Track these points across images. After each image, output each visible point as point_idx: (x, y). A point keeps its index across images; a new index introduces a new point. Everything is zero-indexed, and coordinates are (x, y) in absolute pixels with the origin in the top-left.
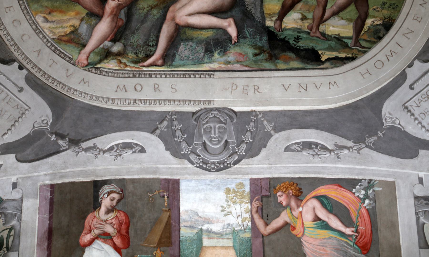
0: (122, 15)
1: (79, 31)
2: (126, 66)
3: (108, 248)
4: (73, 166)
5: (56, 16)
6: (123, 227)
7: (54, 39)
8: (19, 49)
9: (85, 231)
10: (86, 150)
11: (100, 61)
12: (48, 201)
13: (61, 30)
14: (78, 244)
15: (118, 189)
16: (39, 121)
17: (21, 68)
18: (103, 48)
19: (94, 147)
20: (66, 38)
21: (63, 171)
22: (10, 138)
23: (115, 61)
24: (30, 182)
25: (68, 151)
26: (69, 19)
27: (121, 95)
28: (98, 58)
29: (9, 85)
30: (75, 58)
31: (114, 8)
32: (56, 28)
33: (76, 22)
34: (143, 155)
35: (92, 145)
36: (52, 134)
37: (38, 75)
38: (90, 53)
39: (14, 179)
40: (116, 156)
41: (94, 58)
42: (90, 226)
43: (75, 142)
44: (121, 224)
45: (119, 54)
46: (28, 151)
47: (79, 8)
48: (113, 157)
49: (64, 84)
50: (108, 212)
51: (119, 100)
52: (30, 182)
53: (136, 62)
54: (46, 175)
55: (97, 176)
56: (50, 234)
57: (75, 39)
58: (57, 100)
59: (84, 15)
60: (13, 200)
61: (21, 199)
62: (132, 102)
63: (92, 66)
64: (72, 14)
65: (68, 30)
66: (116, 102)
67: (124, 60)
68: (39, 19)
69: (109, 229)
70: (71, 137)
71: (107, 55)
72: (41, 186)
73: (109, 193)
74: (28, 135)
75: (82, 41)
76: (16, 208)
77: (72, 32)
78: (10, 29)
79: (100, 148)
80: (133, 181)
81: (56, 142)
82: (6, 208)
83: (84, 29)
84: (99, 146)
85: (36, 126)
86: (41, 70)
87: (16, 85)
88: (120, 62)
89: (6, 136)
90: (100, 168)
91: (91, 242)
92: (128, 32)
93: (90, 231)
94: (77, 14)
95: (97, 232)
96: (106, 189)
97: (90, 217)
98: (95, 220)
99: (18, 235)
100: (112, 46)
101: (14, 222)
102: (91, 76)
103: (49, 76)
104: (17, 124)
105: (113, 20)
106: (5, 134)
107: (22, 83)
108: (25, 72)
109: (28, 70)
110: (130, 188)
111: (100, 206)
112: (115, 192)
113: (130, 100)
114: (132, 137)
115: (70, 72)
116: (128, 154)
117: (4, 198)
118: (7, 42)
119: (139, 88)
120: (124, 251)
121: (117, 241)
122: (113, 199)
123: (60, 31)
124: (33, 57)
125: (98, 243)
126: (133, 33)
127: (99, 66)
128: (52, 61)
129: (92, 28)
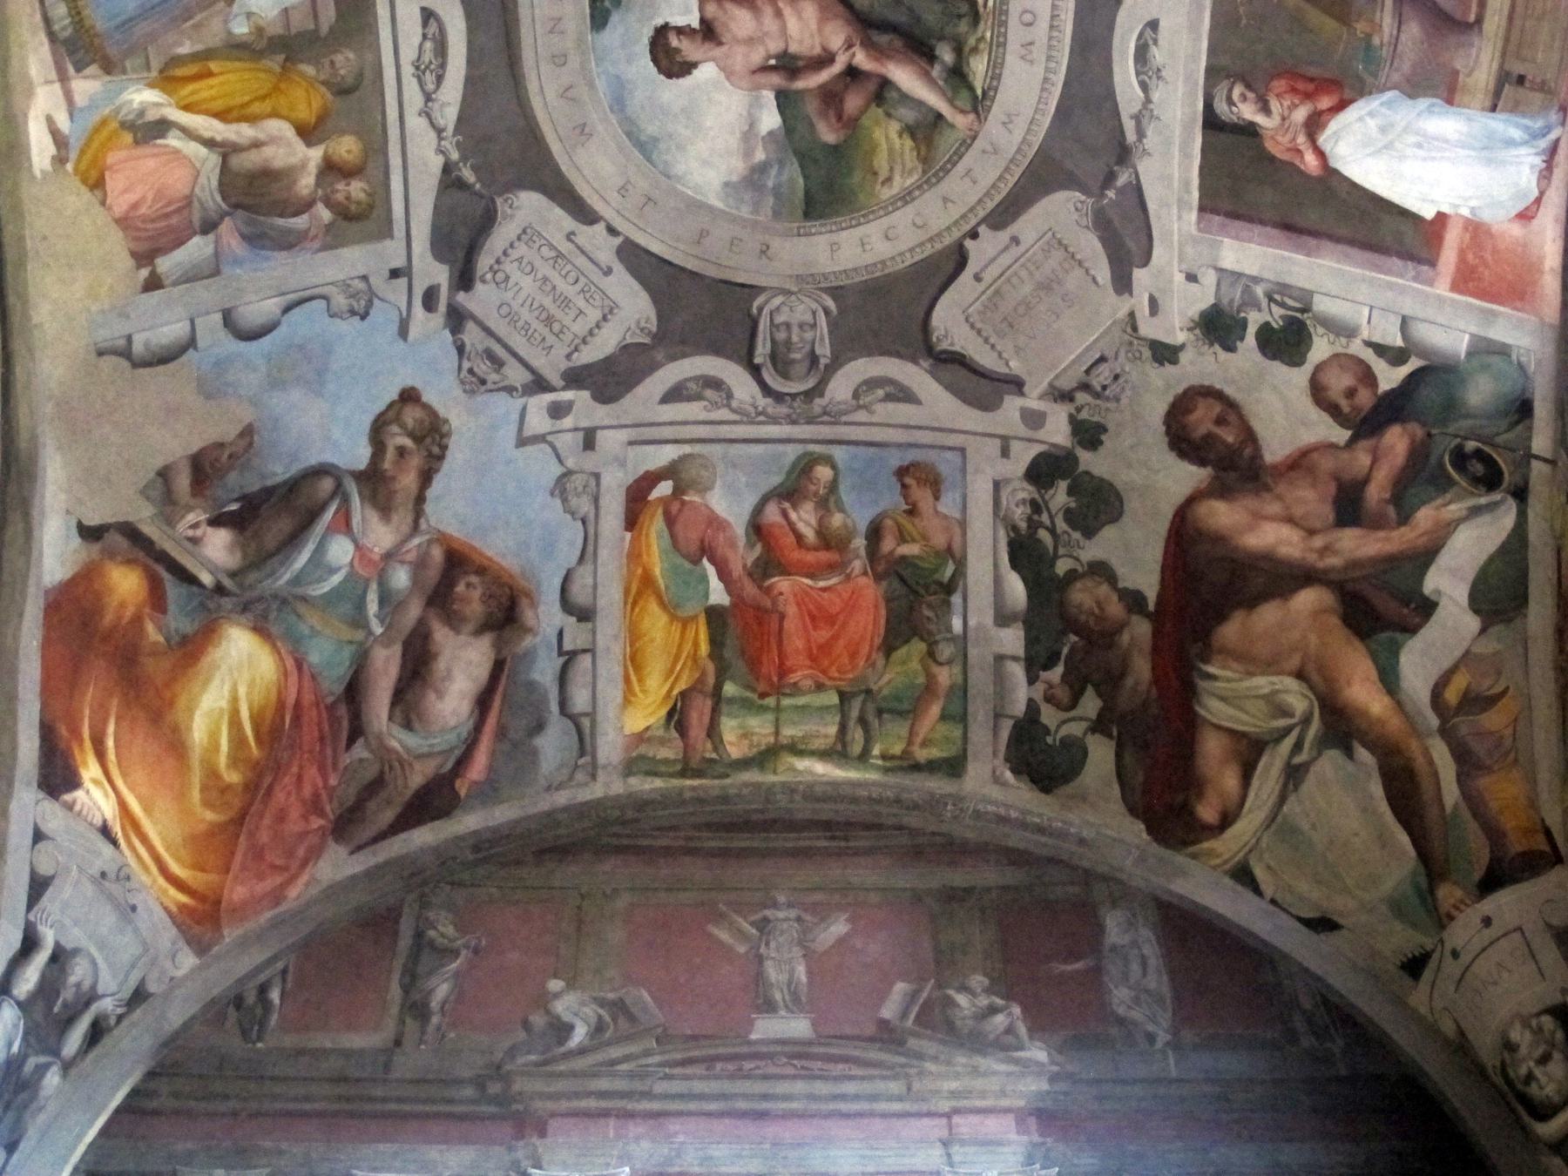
0: (883, 39)
1: (911, 123)
2: (982, 38)
3: (1335, 124)
4: (1170, 168)
5: (881, 162)
6: (1301, 86)
7: (924, 172)
8: (939, 235)
9: (1297, 162)
10: (1141, 134)
11: (971, 89)
12: (1227, 221)
13: (907, 156)
14: (1319, 179)
15: (1225, 84)
16: (1076, 216)
17: (974, 235)
18: (946, 81)
19: (1137, 118)
20: (923, 149)
21: (1176, 184)
22: (1103, 273)
23: (972, 60)
24: (1189, 250)
25: (1140, 169)
26: (887, 137)
27: (1039, 54)
28: (965, 94)
29: (1005, 260)
30: (961, 135)
31: (868, 56)
32: (904, 165)
33: (894, 127)
34: (1162, 24)
35: (1133, 122)
36: (1103, 195)
37: (990, 205)
38: (955, 107)
39: (1179, 278)
40: (1159, 78)
41: (964, 100)
42: (1289, 150)
43: (1124, 154)
44: (1294, 90)
45: (958, 50)
46: (1131, 244)
47: (865, 121)
48: (1161, 84)
49: (1011, 161)
50: (1266, 109)
51: (1049, 58)
52: (1190, 251)
53: (976, 18)
54: (1180, 218)
55: (1194, 120)
56: (1292, 228)
57: (926, 129)
58: (1040, 177)
59: (880, 111)
60: (1218, 284)
61: (1220, 270)
62: (1055, 34)
63: (979, 105)
64: (878, 134)
65: (909, 143)
66: (1053, 65)
67: (972, 41)
68: (886, 193)
69: (1301, 114)
70: (1113, 159)
71: (958, 75)
72: (1200, 230)
73: (1230, 102)
74: (1101, 239)
75: (931, 118)
76: (1233, 284)
77: (913, 137)
78: (903, 246)
79: (1139, 107)
80: (1212, 51)
81: (1120, 191)
82: (1232, 301)
83: (909, 115)
84: (1136, 107)
85: (1084, 222)
86: (980, 201)
87: (1006, 248)
88: (975, 50)
89: (1099, 279)
90: (1179, 113)
91: (1321, 154)
92: (917, 32)
93: (1299, 151)
94: (877, 123)
95: (1301, 139)
96: (1221, 107)
97: (1269, 145)
98: (1279, 138)
99: (1284, 288)
100: (943, 62)
101: (1259, 291)
102: (997, 112)
103: (994, 186)
104: (1078, 257)
105: (889, 57)
106: (1094, 280)
107: (1004, 236)
108: (982, 229)
109: (979, 224)
110: (1224, 61)
111: (1252, 124)
112: (1230, 90)
113: (1050, 38)
114: (1124, 53)
115: (989, 148)
116: (1158, 55)
117: (1212, 301)
118: (926, 254)
119: (1028, 18)
120: (1347, 94)
121: (1325, 103)
122: (1244, 98)
123: (910, 157)
124: (955, 212)
125: (1323, 140)
126: (918, 20)
127: (979, 92)
128: (967, 180)
129: (905, 98)
